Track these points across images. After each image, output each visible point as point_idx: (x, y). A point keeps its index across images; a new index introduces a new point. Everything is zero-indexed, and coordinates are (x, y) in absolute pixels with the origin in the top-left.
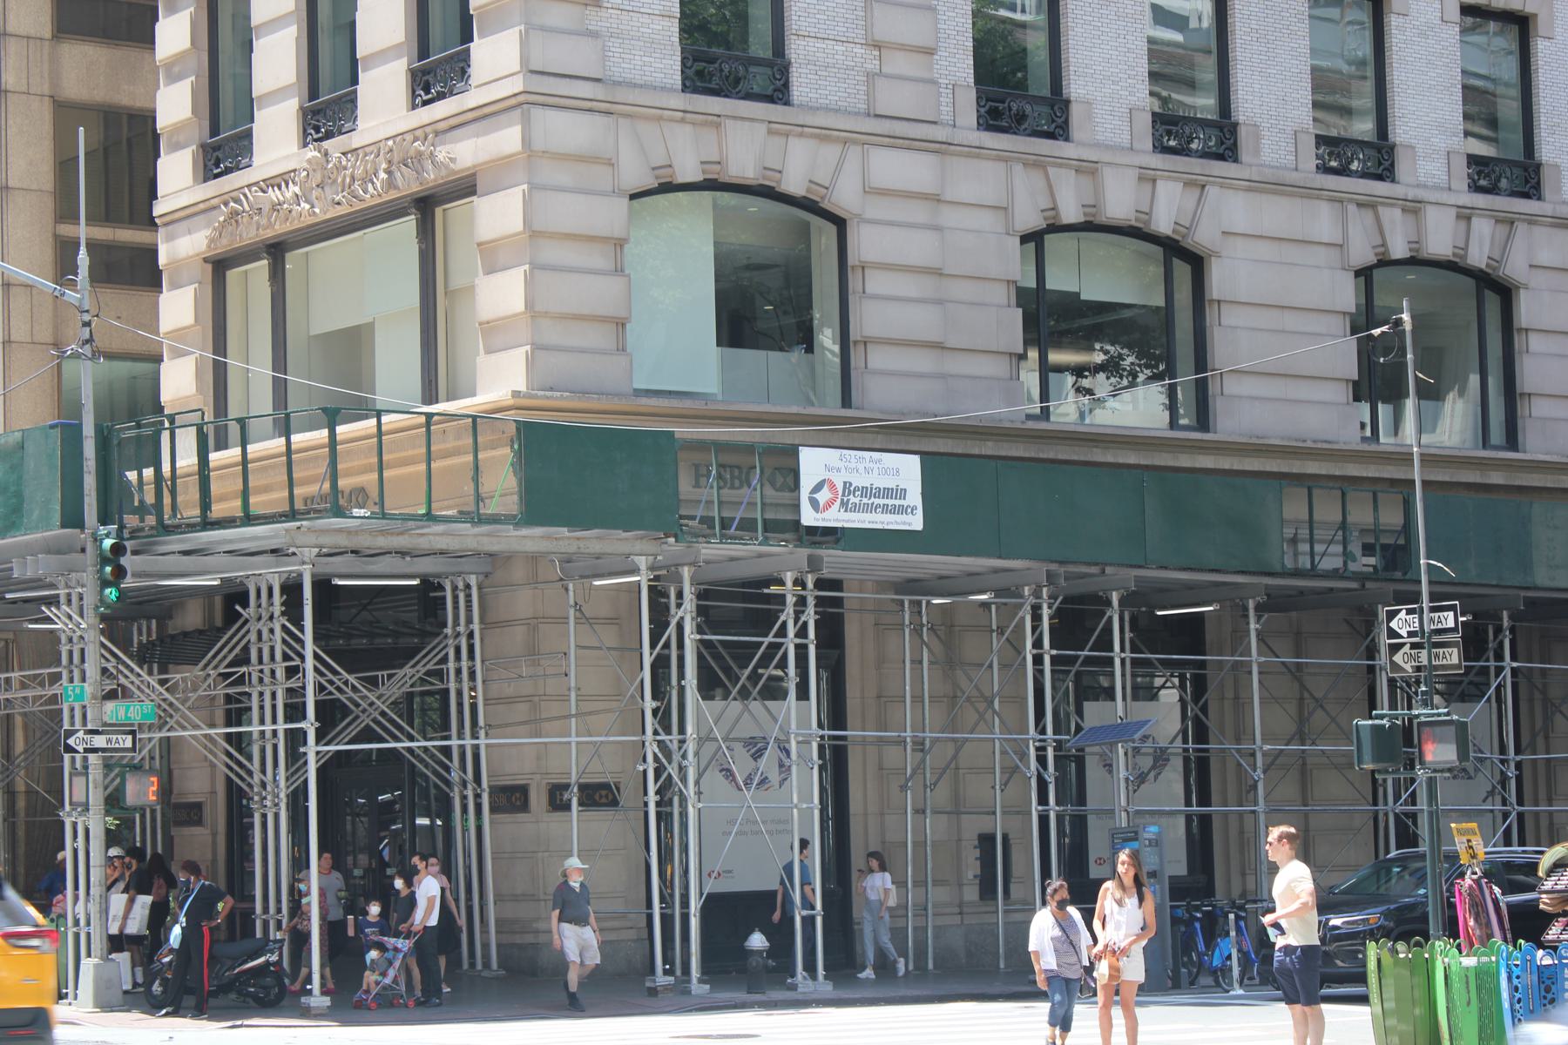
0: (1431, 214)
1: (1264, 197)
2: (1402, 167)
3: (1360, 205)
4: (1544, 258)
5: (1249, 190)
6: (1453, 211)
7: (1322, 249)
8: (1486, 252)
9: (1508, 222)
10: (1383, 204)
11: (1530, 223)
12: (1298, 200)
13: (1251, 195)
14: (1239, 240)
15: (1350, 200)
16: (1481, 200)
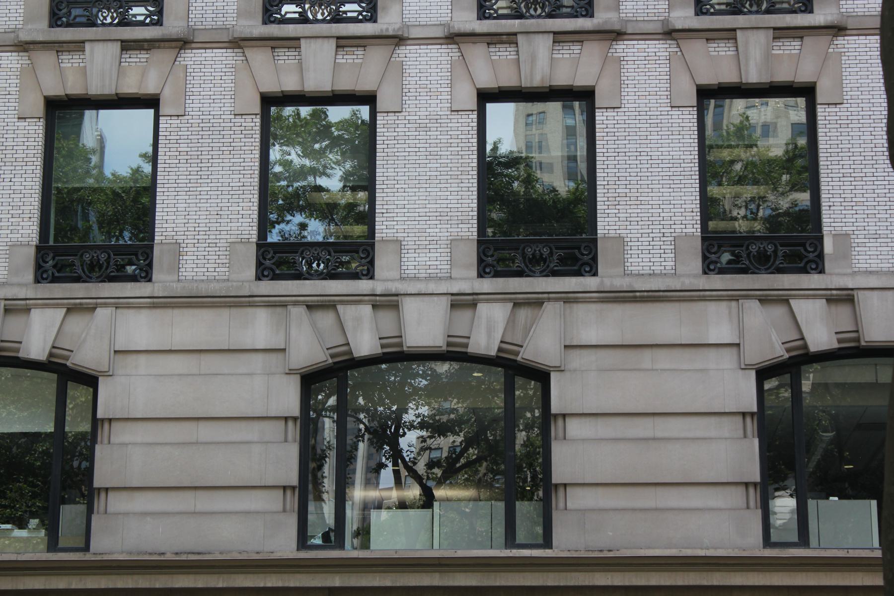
0: (409, 307)
1: (176, 311)
2: (383, 262)
3: (310, 307)
4: (590, 336)
5: (154, 306)
6: (445, 302)
7: (259, 357)
8: (498, 337)
9: (536, 302)
10: (342, 302)
11: (567, 301)
12: (225, 312)
13: (158, 312)
14: (142, 358)
15: (296, 304)
16: (487, 285)
